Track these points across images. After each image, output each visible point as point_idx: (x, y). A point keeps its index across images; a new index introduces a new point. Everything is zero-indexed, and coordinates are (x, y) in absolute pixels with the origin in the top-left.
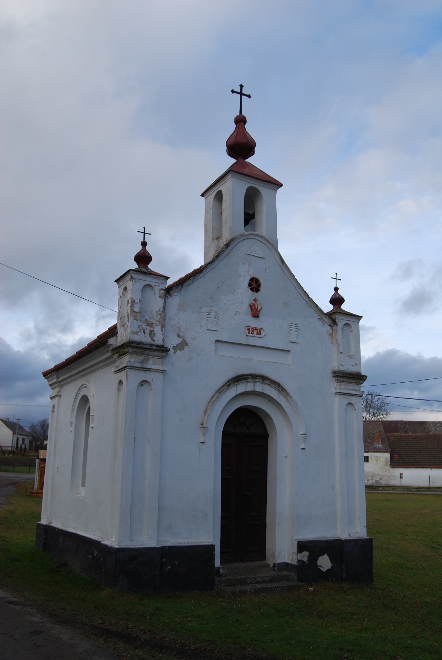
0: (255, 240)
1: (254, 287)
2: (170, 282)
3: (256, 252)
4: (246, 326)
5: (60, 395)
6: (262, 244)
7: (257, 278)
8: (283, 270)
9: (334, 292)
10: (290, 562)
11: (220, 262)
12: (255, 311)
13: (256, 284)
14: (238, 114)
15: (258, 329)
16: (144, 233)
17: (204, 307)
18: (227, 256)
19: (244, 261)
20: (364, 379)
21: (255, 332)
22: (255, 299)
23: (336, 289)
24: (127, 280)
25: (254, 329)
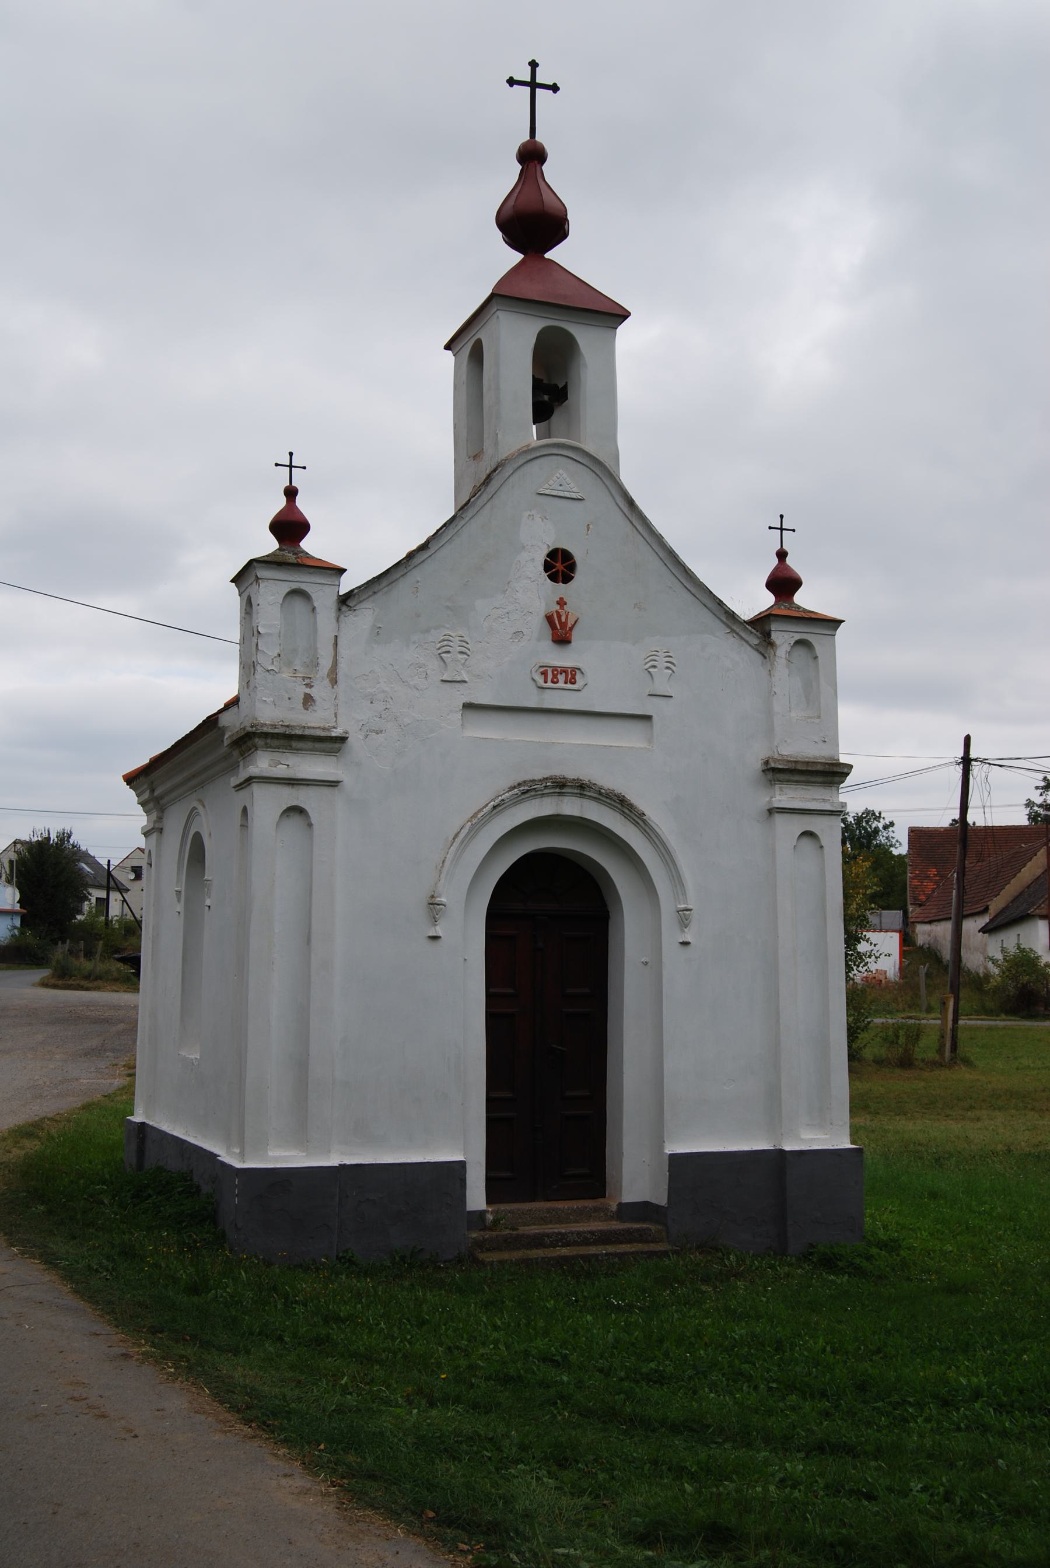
0: (559, 458)
1: (558, 571)
2: (347, 584)
3: (561, 488)
4: (537, 666)
5: (162, 829)
6: (579, 465)
7: (564, 548)
8: (633, 524)
9: (776, 561)
10: (654, 1201)
11: (471, 519)
12: (559, 628)
13: (562, 564)
14: (526, 137)
15: (569, 670)
16: (291, 466)
17: (432, 630)
18: (489, 503)
19: (533, 512)
20: (843, 773)
21: (561, 678)
22: (561, 599)
23: (782, 555)
24: (250, 582)
25: (557, 671)
